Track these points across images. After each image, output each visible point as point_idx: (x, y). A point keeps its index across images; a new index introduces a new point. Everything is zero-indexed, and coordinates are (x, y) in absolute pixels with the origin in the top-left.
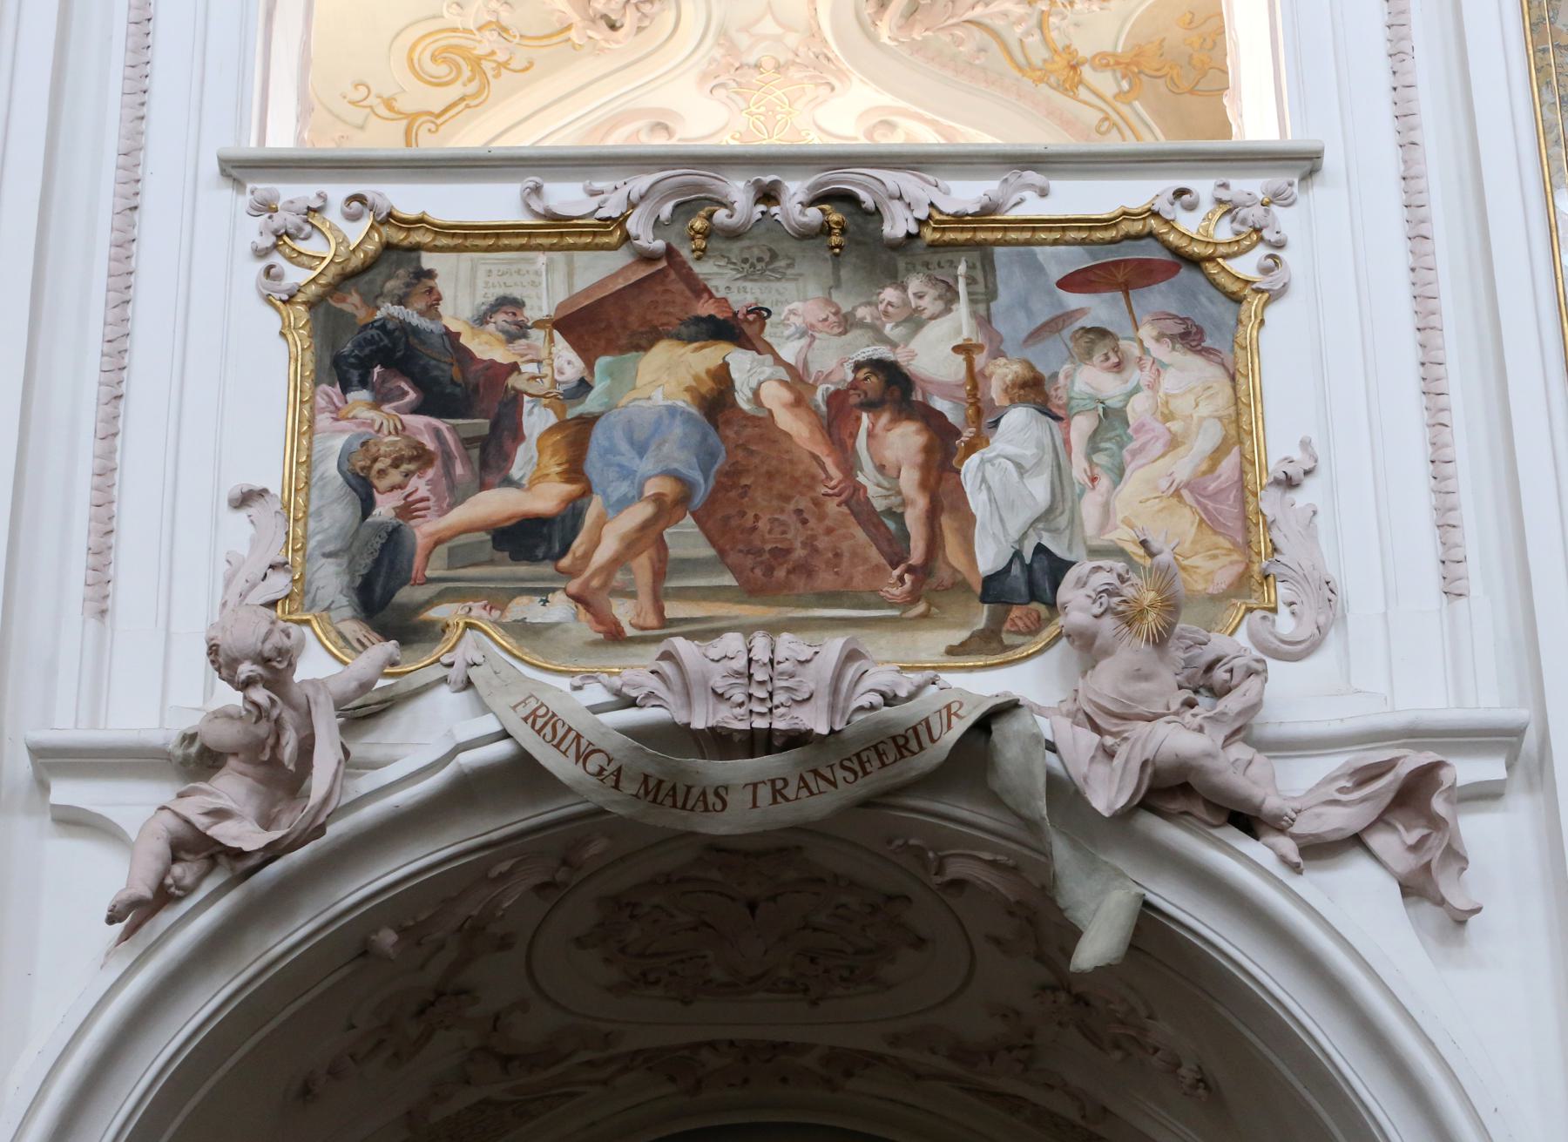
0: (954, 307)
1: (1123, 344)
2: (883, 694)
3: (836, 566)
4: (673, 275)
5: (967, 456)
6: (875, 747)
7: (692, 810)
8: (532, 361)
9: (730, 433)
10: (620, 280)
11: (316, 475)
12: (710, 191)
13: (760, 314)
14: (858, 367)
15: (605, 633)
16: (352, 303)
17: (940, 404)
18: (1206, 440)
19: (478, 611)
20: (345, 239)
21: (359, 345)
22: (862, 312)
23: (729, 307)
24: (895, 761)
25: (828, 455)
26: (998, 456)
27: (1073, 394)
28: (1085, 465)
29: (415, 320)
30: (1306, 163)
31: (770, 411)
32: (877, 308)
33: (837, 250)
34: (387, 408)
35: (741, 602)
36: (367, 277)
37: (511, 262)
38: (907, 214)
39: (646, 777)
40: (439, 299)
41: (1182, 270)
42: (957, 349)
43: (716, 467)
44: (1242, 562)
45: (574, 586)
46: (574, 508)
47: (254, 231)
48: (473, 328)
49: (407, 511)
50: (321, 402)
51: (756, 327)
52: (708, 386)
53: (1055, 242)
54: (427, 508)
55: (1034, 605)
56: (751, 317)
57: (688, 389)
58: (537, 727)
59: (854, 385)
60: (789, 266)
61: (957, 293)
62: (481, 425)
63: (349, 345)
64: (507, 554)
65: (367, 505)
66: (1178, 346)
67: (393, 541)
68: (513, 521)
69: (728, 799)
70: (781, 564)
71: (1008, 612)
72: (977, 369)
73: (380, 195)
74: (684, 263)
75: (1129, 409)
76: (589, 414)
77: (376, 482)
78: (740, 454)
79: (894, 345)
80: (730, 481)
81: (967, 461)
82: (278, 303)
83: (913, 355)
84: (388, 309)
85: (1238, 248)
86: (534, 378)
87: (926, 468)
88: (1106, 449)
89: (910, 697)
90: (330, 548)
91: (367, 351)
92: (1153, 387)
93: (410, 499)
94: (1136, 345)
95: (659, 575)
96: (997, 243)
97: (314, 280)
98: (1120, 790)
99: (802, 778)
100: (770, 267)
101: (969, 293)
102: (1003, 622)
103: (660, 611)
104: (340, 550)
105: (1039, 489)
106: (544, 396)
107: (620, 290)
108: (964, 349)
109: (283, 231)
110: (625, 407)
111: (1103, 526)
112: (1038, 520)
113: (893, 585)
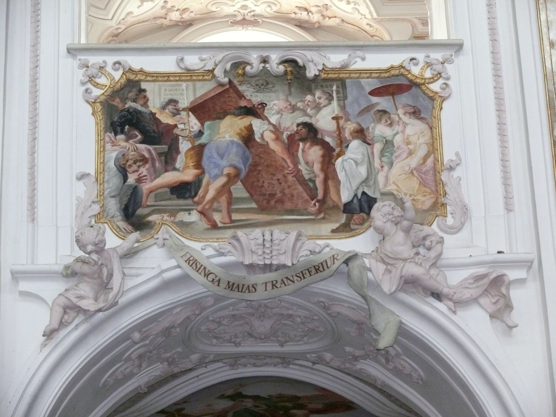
0: (332, 102)
1: (392, 116)
2: (310, 251)
3: (292, 200)
4: (231, 91)
5: (337, 159)
6: (308, 269)
7: (244, 292)
8: (182, 123)
9: (253, 150)
10: (213, 93)
11: (106, 167)
12: (243, 59)
13: (263, 105)
14: (298, 125)
15: (211, 225)
16: (117, 102)
17: (328, 139)
18: (422, 152)
19: (166, 217)
20: (114, 78)
21: (120, 118)
22: (299, 105)
23: (252, 103)
24: (315, 274)
25: (288, 159)
26: (349, 158)
27: (375, 135)
28: (379, 161)
29: (139, 108)
30: (458, 47)
31: (267, 142)
32: (304, 102)
33: (290, 81)
34: (131, 141)
35: (259, 214)
36: (122, 92)
37: (173, 86)
38: (315, 67)
39: (229, 282)
40: (148, 100)
41: (413, 88)
42: (333, 118)
43: (249, 163)
45: (200, 208)
46: (199, 179)
47: (80, 75)
48: (160, 111)
49: (139, 180)
50: (107, 139)
51: (261, 110)
52: (245, 133)
53: (368, 78)
54: (147, 179)
55: (362, 214)
56: (260, 106)
57: (238, 134)
58: (190, 264)
59: (297, 132)
60: (273, 87)
61: (333, 97)
63: (116, 118)
64: (175, 196)
65: (125, 178)
66: (412, 117)
67: (135, 191)
68: (178, 184)
70: (272, 199)
71: (352, 217)
72: (340, 126)
73: (126, 61)
74: (235, 86)
75: (394, 140)
76: (203, 143)
77: (128, 169)
78: (257, 158)
79: (311, 117)
80: (254, 168)
81: (337, 161)
83: (318, 121)
84: (130, 104)
85: (433, 80)
86: (183, 130)
88: (386, 156)
89: (320, 252)
90: (113, 194)
91: (123, 120)
92: (403, 132)
93: (140, 176)
94: (397, 116)
95: (230, 203)
96: (347, 78)
97: (103, 94)
99: (282, 280)
101: (337, 97)
102: (350, 221)
103: (230, 217)
104: (117, 195)
105: (363, 171)
106: (186, 137)
107: (213, 96)
108: (336, 118)
109: (91, 76)
110: (216, 141)
111: (386, 185)
112: (363, 182)
113: (312, 207)
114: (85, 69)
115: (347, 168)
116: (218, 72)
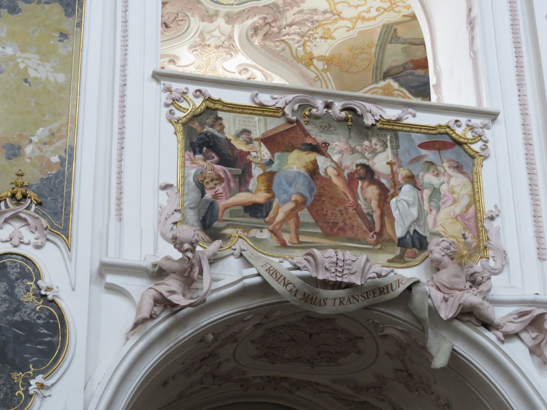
0: (386, 149)
1: (438, 168)
2: (377, 274)
3: (353, 229)
4: (298, 129)
6: (373, 291)
7: (316, 305)
8: (254, 151)
9: (318, 182)
10: (282, 128)
11: (186, 181)
12: (310, 102)
13: (326, 144)
14: (357, 165)
15: (281, 244)
16: (196, 125)
17: (383, 181)
18: (464, 202)
19: (240, 232)
21: (198, 140)
22: (358, 148)
23: (316, 141)
24: (378, 295)
25: (349, 193)
26: (401, 200)
27: (424, 182)
28: (428, 205)
29: (216, 133)
31: (330, 177)
32: (363, 146)
33: (350, 127)
34: (208, 161)
36: (200, 117)
37: (247, 118)
38: (372, 118)
39: (305, 293)
40: (224, 127)
42: (388, 163)
43: (314, 193)
44: (476, 242)
45: (270, 227)
46: (269, 202)
48: (235, 138)
49: (216, 196)
50: (187, 157)
51: (325, 148)
52: (310, 166)
53: (418, 132)
54: (223, 196)
55: (414, 249)
56: (323, 145)
57: (304, 167)
58: (271, 273)
59: (356, 171)
60: (335, 130)
61: (387, 145)
62: (239, 171)
63: (195, 139)
64: (248, 214)
65: (203, 193)
66: (455, 170)
68: (250, 204)
69: (326, 302)
70: (336, 227)
71: (406, 251)
72: (394, 171)
73: (206, 90)
74: (302, 125)
75: (441, 189)
76: (273, 171)
77: (206, 186)
78: (322, 190)
79: (368, 160)
80: (319, 198)
81: (392, 200)
82: (174, 123)
83: (374, 164)
84: (207, 129)
85: (474, 141)
86: (255, 157)
87: (379, 201)
88: (434, 201)
89: (385, 276)
90: (191, 206)
91: (201, 142)
92: (448, 182)
93: (217, 193)
94: (442, 168)
96: (399, 130)
97: (185, 116)
98: (450, 312)
99: (349, 298)
100: (329, 130)
101: (391, 146)
102: (405, 253)
103: (298, 239)
104: (194, 207)
105: (414, 211)
106: (259, 164)
107: (282, 131)
108: (390, 164)
109: (175, 99)
110: (285, 170)
112: (414, 222)
113: (370, 238)
114: (168, 93)
115: (401, 207)
116: (287, 110)
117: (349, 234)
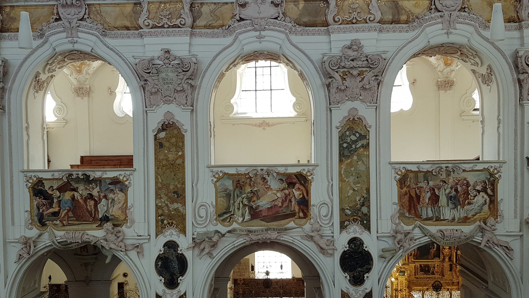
13: (78, 188)
14: (87, 194)
16: (36, 187)
17: (96, 198)
29: (43, 189)
42: (98, 192)
45: (60, 220)
49: (43, 211)
62: (50, 201)
65: (39, 210)
67: (42, 214)
84: (40, 187)
87: (94, 206)
92: (117, 196)
95: (68, 218)
105: (106, 208)
111: (112, 212)
115: (101, 207)
117: (84, 219)
